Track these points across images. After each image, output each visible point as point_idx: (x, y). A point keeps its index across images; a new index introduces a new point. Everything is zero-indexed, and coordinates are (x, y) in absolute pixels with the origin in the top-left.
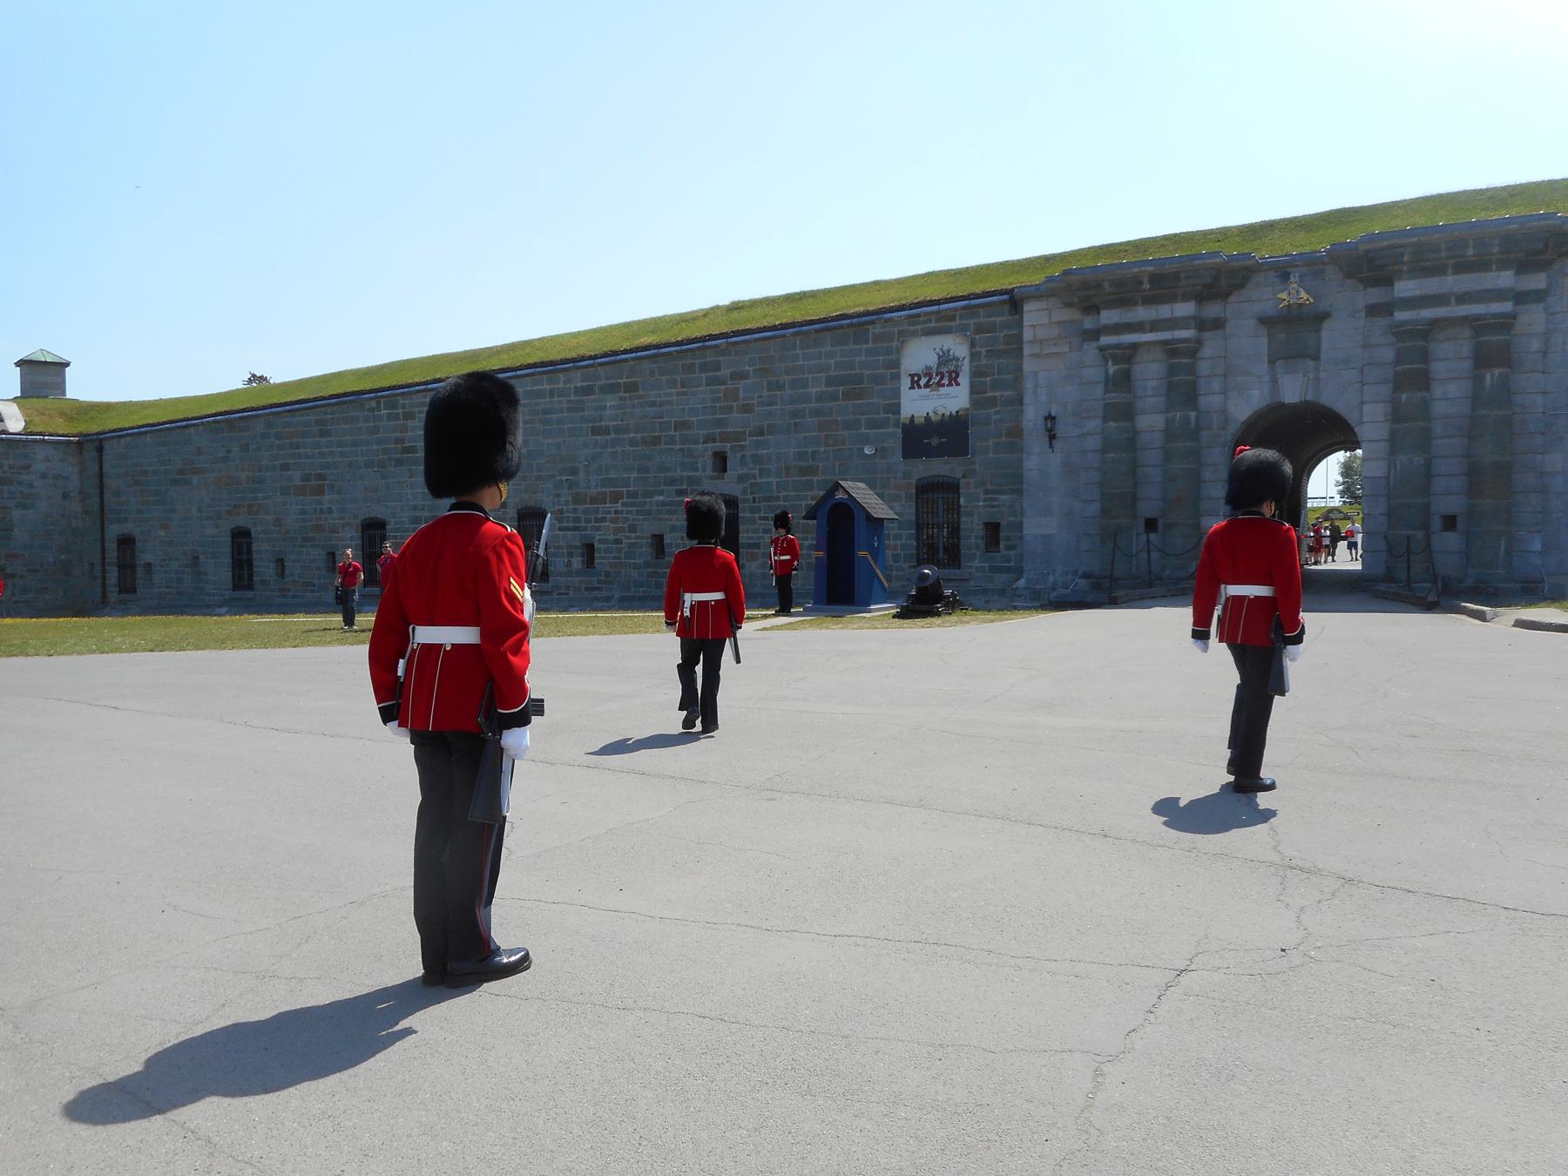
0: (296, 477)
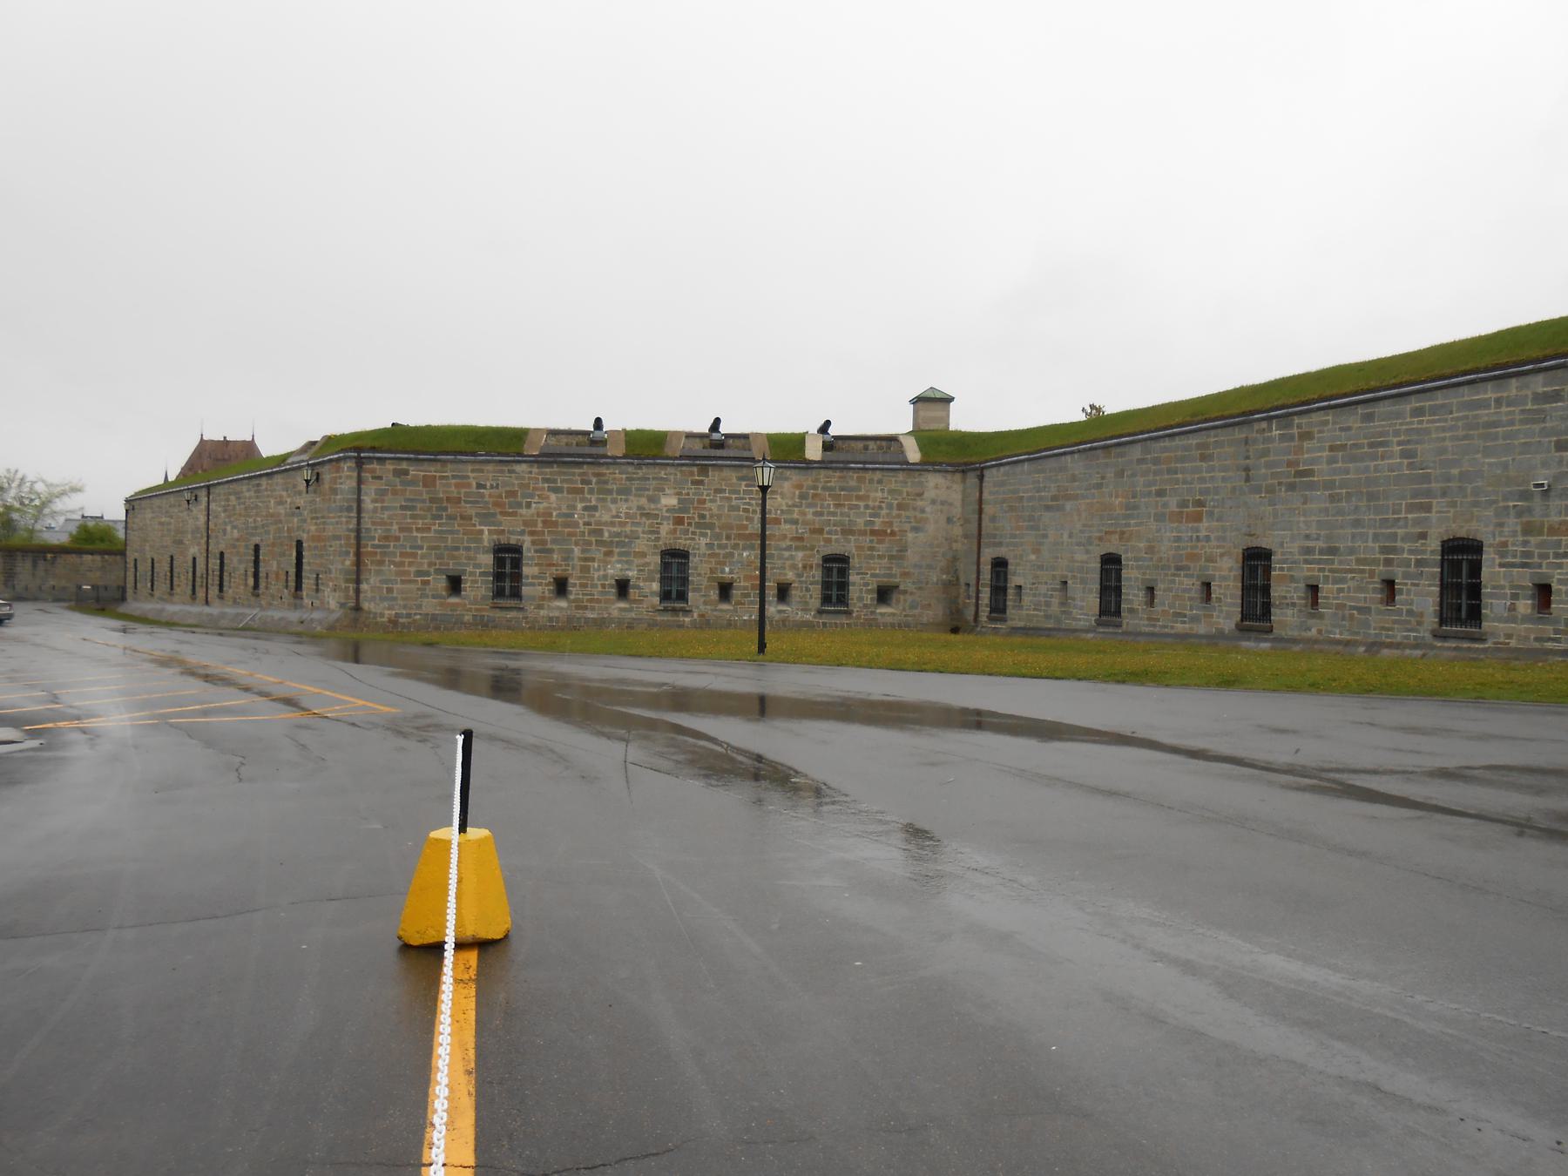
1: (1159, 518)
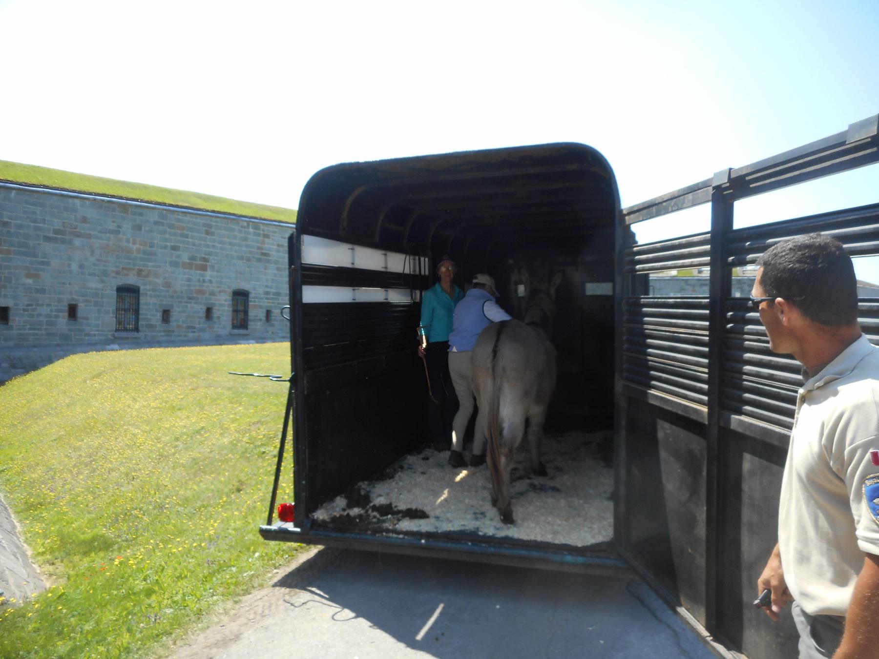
0: (185, 258)
1: (174, 264)
